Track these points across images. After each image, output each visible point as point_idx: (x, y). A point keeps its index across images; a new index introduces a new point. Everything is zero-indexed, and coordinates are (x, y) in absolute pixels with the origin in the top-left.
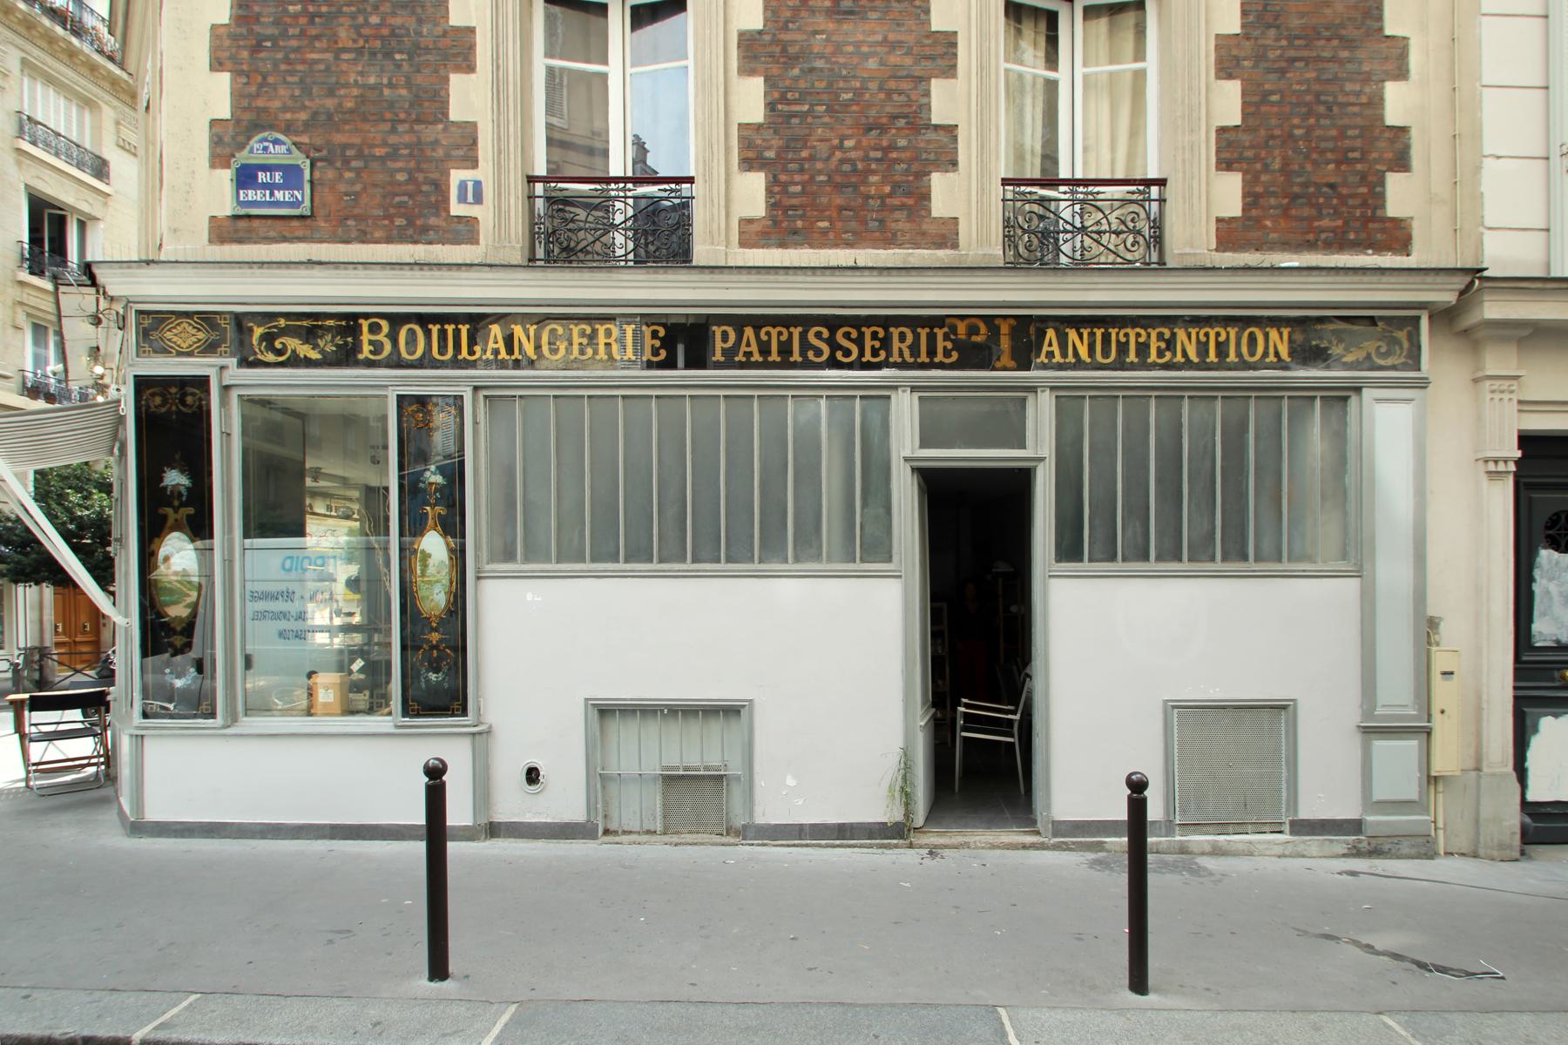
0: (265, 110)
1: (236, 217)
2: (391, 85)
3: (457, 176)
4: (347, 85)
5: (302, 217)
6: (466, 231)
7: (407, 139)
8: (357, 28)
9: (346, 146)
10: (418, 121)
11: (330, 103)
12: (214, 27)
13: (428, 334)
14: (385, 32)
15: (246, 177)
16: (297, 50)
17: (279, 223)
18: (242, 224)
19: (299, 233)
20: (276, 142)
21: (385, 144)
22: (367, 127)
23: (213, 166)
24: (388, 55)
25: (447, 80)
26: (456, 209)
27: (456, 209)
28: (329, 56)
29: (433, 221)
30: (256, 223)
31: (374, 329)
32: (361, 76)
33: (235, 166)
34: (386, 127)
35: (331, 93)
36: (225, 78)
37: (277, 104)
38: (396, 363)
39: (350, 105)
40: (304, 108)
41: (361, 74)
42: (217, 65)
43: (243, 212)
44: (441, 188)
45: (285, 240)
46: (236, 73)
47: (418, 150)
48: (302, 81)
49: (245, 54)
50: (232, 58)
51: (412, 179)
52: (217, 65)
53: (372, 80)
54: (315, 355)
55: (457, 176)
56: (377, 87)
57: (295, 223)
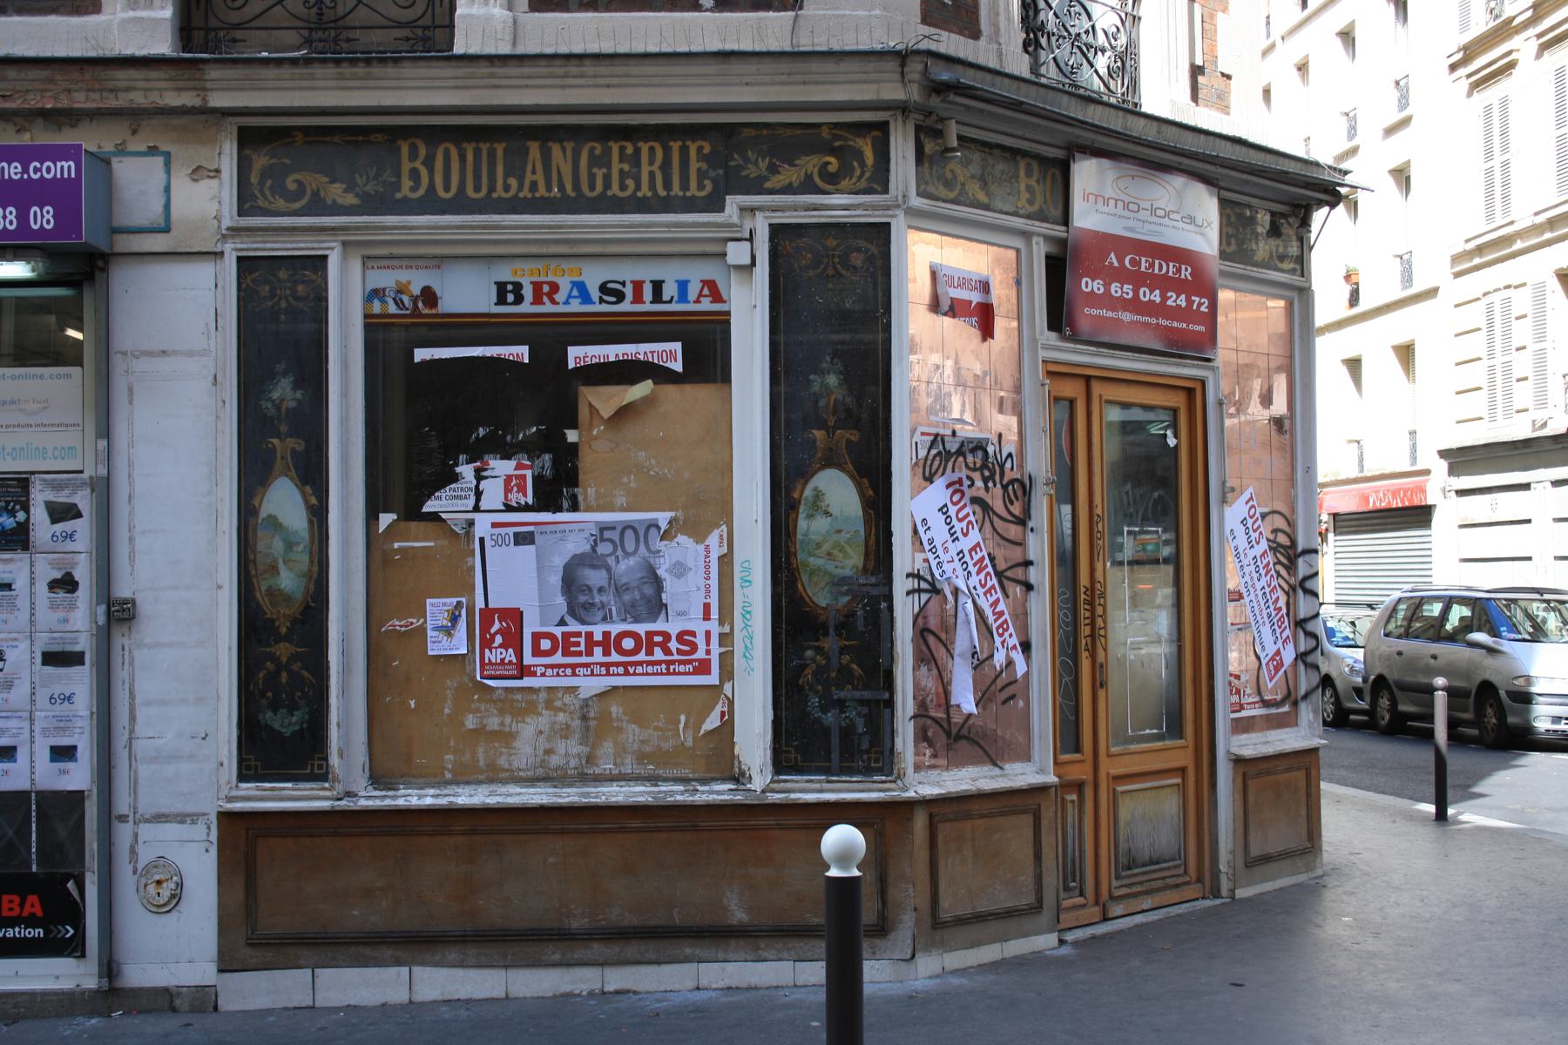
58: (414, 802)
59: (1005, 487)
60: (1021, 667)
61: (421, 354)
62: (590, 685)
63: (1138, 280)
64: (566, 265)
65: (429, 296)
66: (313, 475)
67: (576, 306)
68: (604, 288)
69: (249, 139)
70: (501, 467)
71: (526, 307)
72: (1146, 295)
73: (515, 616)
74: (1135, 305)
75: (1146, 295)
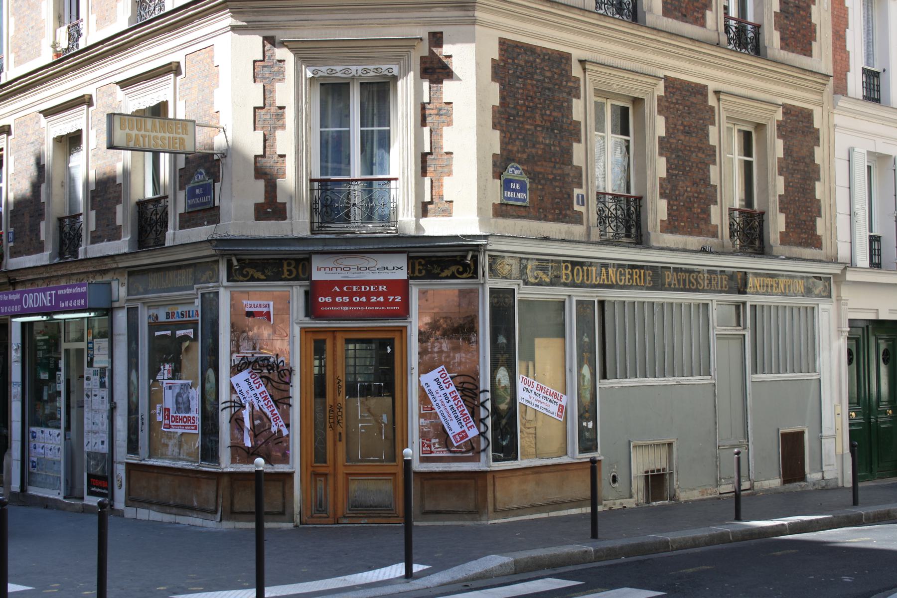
0: (511, 151)
1: (501, 204)
2: (554, 145)
3: (577, 191)
4: (539, 143)
5: (525, 207)
6: (577, 219)
7: (559, 172)
8: (542, 115)
9: (540, 173)
10: (563, 164)
11: (534, 151)
12: (494, 106)
13: (583, 271)
14: (552, 119)
15: (506, 185)
16: (522, 123)
17: (517, 209)
18: (504, 208)
19: (524, 214)
20: (517, 168)
21: (552, 173)
22: (545, 163)
23: (494, 178)
24: (553, 130)
25: (572, 145)
26: (577, 208)
27: (577, 208)
28: (532, 127)
29: (568, 212)
30: (509, 208)
31: (567, 268)
32: (543, 138)
33: (503, 179)
34: (552, 165)
35: (534, 146)
36: (498, 132)
37: (515, 149)
38: (574, 285)
39: (540, 152)
40: (524, 152)
41: (544, 138)
42: (495, 127)
43: (506, 202)
44: (570, 196)
45: (519, 217)
46: (502, 131)
47: (564, 176)
48: (524, 139)
49: (504, 122)
50: (499, 123)
51: (561, 191)
52: (495, 127)
53: (547, 142)
54: (548, 280)
55: (577, 191)
56: (549, 145)
57: (522, 209)
58: (156, 464)
59: (279, 372)
60: (285, 432)
61: (157, 334)
62: (180, 431)
63: (351, 294)
64: (176, 306)
65: (157, 317)
66: (137, 370)
67: (177, 319)
68: (182, 314)
69: (130, 274)
70: (167, 366)
71: (170, 320)
72: (356, 299)
73: (168, 410)
74: (351, 303)
75: (356, 299)
